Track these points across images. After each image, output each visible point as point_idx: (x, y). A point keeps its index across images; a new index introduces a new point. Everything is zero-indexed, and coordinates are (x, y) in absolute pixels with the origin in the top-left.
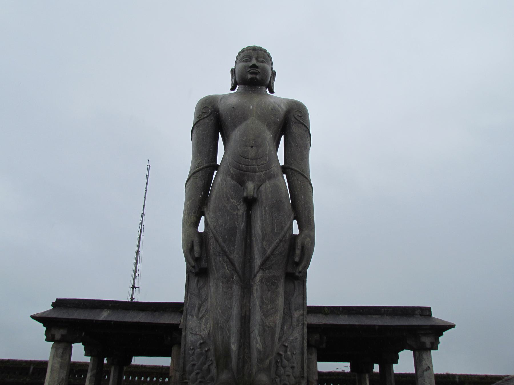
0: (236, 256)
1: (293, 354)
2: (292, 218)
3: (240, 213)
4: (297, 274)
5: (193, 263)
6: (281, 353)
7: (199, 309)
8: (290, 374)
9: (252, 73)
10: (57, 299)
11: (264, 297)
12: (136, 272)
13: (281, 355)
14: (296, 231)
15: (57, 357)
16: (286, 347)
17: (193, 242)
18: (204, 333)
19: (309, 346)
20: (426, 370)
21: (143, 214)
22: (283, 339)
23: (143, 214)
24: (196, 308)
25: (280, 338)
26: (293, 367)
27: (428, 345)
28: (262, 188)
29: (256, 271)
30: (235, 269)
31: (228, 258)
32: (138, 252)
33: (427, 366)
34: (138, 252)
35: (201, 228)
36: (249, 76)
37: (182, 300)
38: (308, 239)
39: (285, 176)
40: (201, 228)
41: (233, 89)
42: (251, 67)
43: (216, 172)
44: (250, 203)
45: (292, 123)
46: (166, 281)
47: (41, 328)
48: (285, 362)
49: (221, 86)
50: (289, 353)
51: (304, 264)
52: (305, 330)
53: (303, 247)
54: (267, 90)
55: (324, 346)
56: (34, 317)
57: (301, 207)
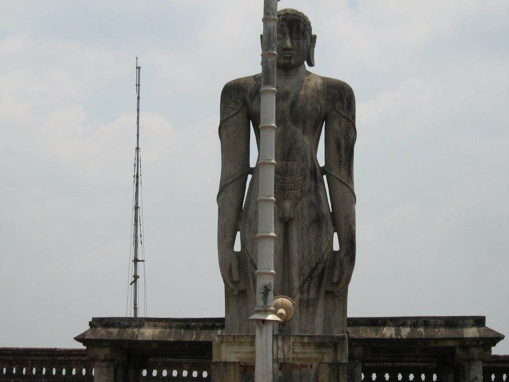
5: (231, 286)
10: (93, 319)
11: (302, 319)
14: (336, 247)
15: (103, 375)
17: (230, 265)
21: (138, 149)
23: (138, 149)
24: (238, 328)
32: (137, 208)
33: (474, 377)
34: (137, 208)
35: (237, 247)
40: (237, 247)
45: (337, 104)
51: (342, 284)
54: (306, 63)
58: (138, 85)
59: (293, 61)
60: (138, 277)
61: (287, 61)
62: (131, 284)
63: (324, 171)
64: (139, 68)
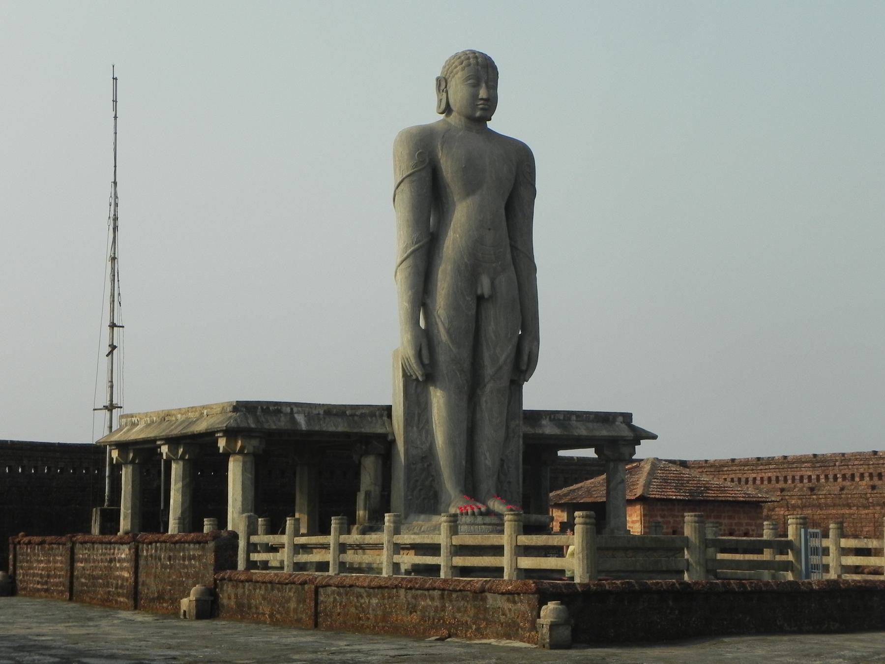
20: (620, 483)
23: (115, 183)
24: (416, 418)
26: (509, 483)
29: (486, 380)
32: (113, 259)
35: (422, 324)
58: (115, 101)
60: (115, 347)
62: (107, 356)
64: (116, 79)
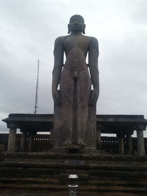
0: (71, 98)
1: (91, 131)
2: (91, 83)
3: (72, 83)
4: (93, 104)
5: (56, 101)
6: (87, 131)
7: (59, 117)
8: (91, 138)
9: (76, 27)
12: (36, 101)
13: (87, 132)
14: (92, 89)
16: (89, 129)
17: (56, 94)
18: (61, 125)
19: (97, 129)
20: (141, 137)
21: (38, 79)
22: (88, 126)
23: (38, 79)
25: (87, 126)
26: (91, 136)
27: (142, 129)
28: (80, 73)
29: (78, 103)
30: (71, 104)
31: (68, 99)
32: (37, 94)
34: (37, 94)
35: (59, 88)
36: (75, 28)
37: (53, 114)
38: (97, 92)
39: (88, 68)
40: (59, 88)
41: (69, 33)
42: (75, 24)
43: (63, 67)
44: (75, 79)
45: (91, 46)
46: (47, 106)
47: (5, 124)
48: (89, 134)
49: (65, 33)
50: (90, 131)
52: (96, 123)
53: (95, 94)
55: (103, 129)
56: (2, 120)
57: (95, 80)
58: (38, 64)
59: (78, 28)
61: (76, 28)
63: (88, 65)
